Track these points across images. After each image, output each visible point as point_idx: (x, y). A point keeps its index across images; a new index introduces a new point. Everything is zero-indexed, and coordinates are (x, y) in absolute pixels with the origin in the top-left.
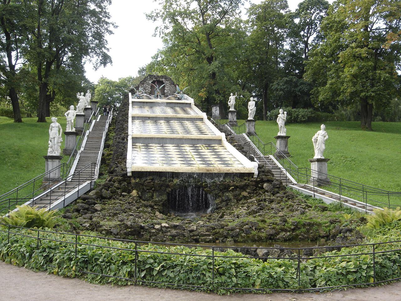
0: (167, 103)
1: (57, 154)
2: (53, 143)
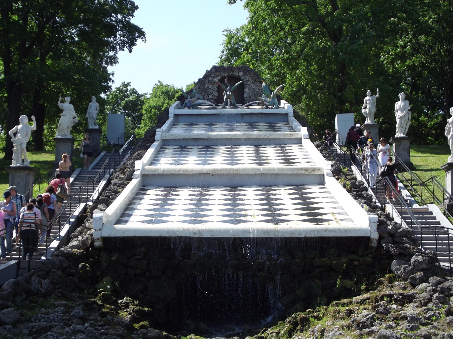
0: (242, 115)
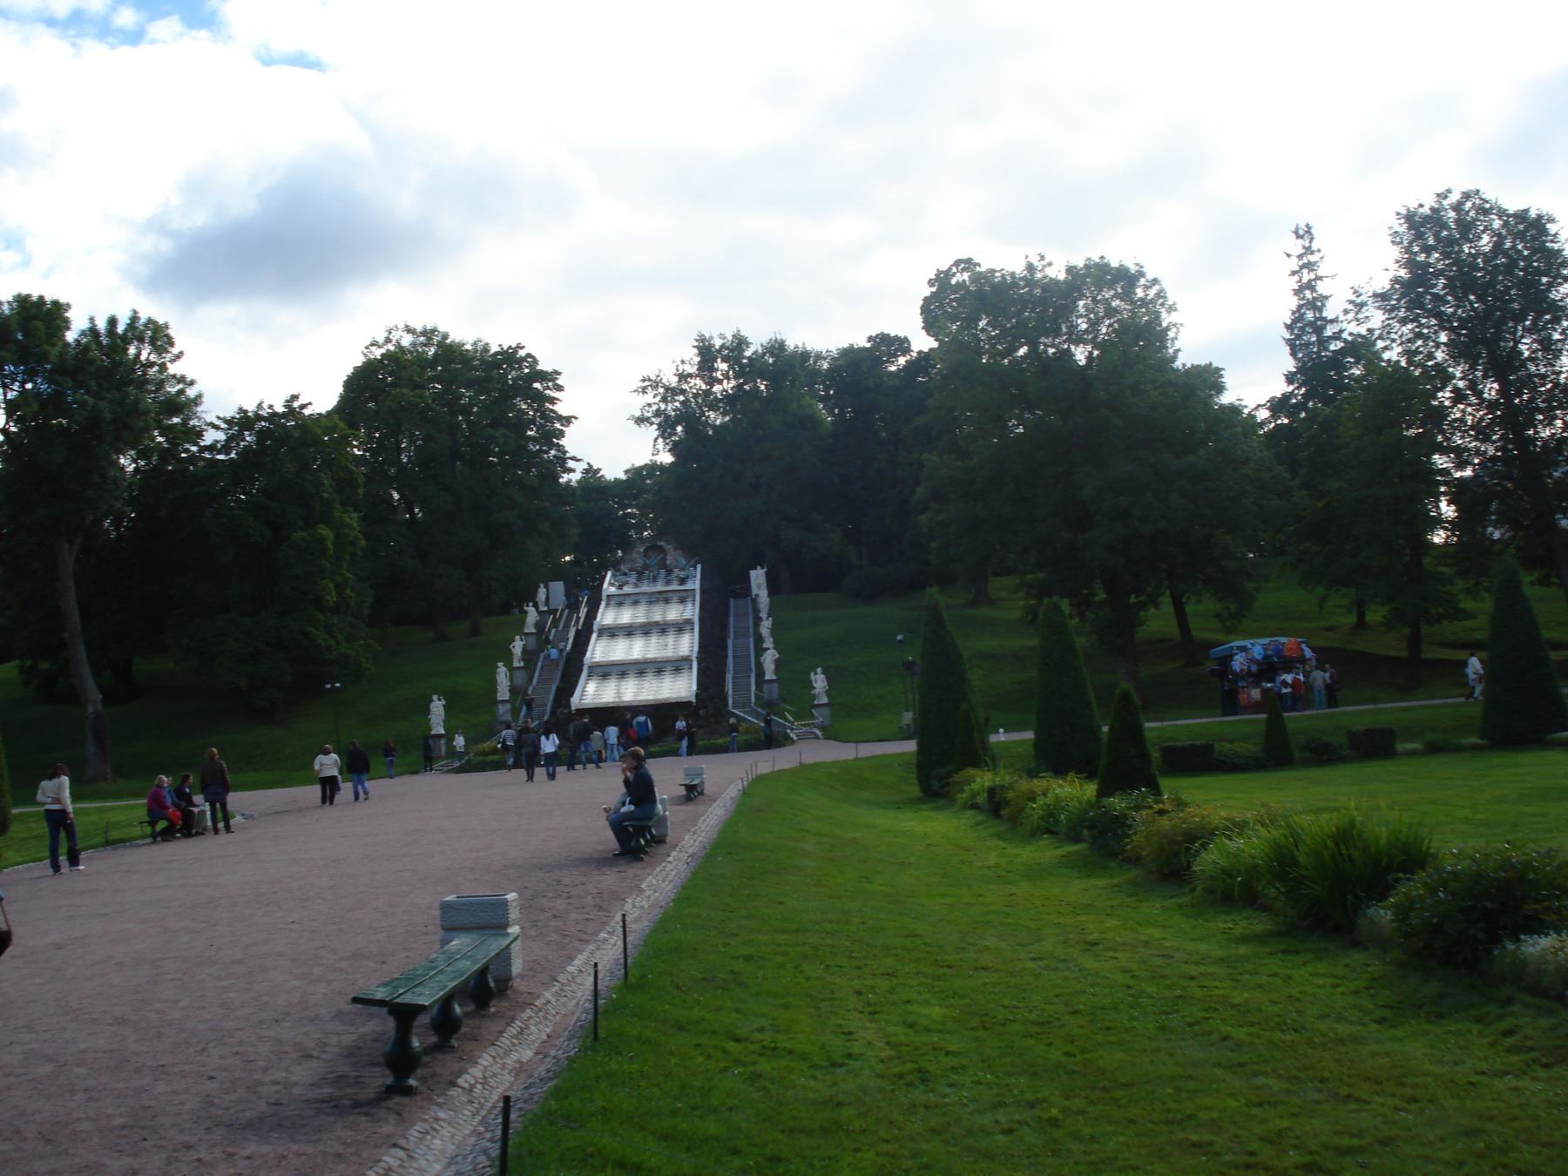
1: (507, 697)
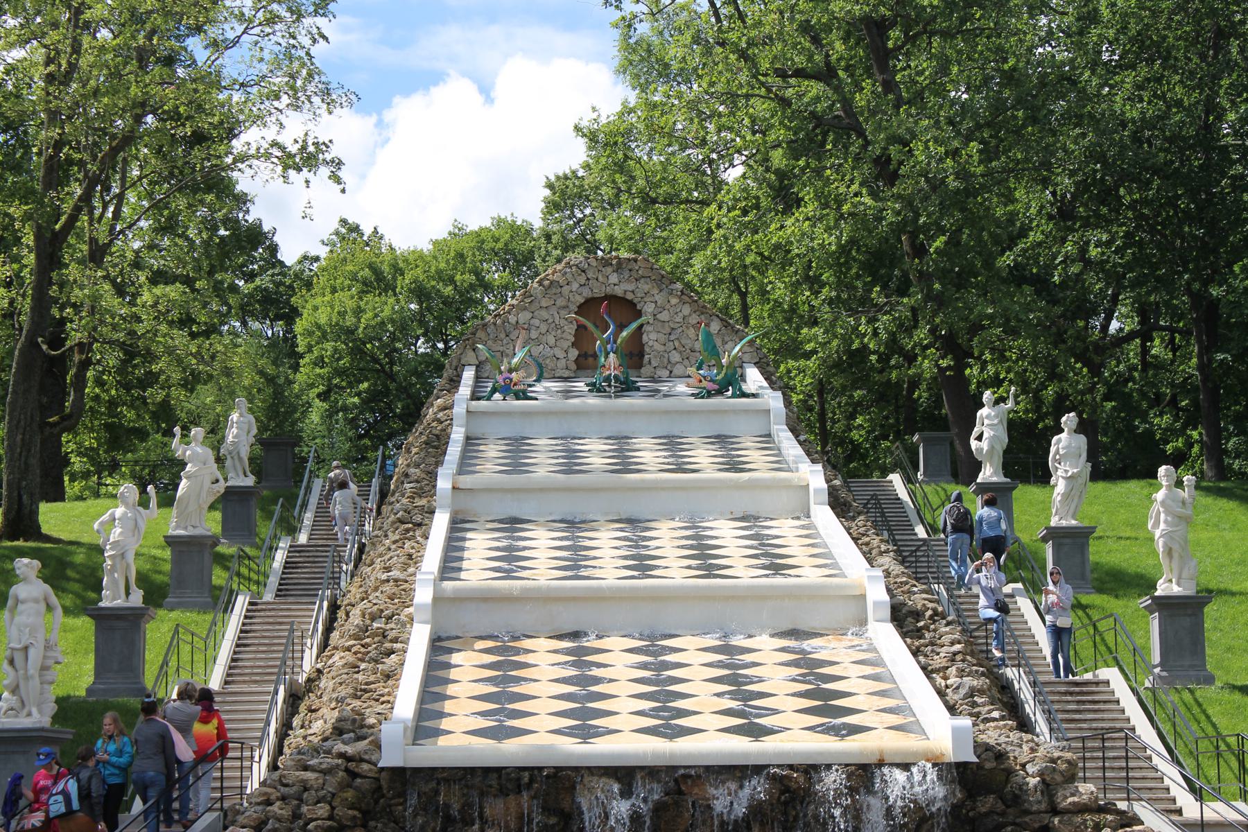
2: (21, 672)
